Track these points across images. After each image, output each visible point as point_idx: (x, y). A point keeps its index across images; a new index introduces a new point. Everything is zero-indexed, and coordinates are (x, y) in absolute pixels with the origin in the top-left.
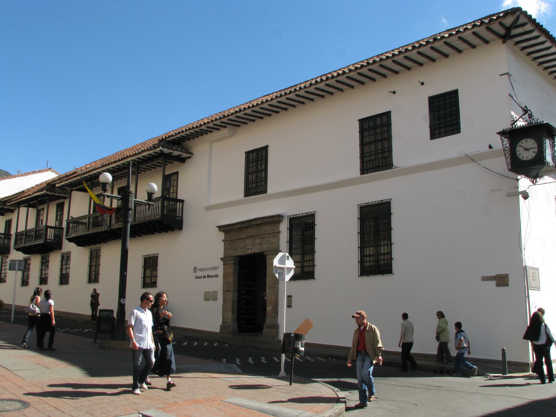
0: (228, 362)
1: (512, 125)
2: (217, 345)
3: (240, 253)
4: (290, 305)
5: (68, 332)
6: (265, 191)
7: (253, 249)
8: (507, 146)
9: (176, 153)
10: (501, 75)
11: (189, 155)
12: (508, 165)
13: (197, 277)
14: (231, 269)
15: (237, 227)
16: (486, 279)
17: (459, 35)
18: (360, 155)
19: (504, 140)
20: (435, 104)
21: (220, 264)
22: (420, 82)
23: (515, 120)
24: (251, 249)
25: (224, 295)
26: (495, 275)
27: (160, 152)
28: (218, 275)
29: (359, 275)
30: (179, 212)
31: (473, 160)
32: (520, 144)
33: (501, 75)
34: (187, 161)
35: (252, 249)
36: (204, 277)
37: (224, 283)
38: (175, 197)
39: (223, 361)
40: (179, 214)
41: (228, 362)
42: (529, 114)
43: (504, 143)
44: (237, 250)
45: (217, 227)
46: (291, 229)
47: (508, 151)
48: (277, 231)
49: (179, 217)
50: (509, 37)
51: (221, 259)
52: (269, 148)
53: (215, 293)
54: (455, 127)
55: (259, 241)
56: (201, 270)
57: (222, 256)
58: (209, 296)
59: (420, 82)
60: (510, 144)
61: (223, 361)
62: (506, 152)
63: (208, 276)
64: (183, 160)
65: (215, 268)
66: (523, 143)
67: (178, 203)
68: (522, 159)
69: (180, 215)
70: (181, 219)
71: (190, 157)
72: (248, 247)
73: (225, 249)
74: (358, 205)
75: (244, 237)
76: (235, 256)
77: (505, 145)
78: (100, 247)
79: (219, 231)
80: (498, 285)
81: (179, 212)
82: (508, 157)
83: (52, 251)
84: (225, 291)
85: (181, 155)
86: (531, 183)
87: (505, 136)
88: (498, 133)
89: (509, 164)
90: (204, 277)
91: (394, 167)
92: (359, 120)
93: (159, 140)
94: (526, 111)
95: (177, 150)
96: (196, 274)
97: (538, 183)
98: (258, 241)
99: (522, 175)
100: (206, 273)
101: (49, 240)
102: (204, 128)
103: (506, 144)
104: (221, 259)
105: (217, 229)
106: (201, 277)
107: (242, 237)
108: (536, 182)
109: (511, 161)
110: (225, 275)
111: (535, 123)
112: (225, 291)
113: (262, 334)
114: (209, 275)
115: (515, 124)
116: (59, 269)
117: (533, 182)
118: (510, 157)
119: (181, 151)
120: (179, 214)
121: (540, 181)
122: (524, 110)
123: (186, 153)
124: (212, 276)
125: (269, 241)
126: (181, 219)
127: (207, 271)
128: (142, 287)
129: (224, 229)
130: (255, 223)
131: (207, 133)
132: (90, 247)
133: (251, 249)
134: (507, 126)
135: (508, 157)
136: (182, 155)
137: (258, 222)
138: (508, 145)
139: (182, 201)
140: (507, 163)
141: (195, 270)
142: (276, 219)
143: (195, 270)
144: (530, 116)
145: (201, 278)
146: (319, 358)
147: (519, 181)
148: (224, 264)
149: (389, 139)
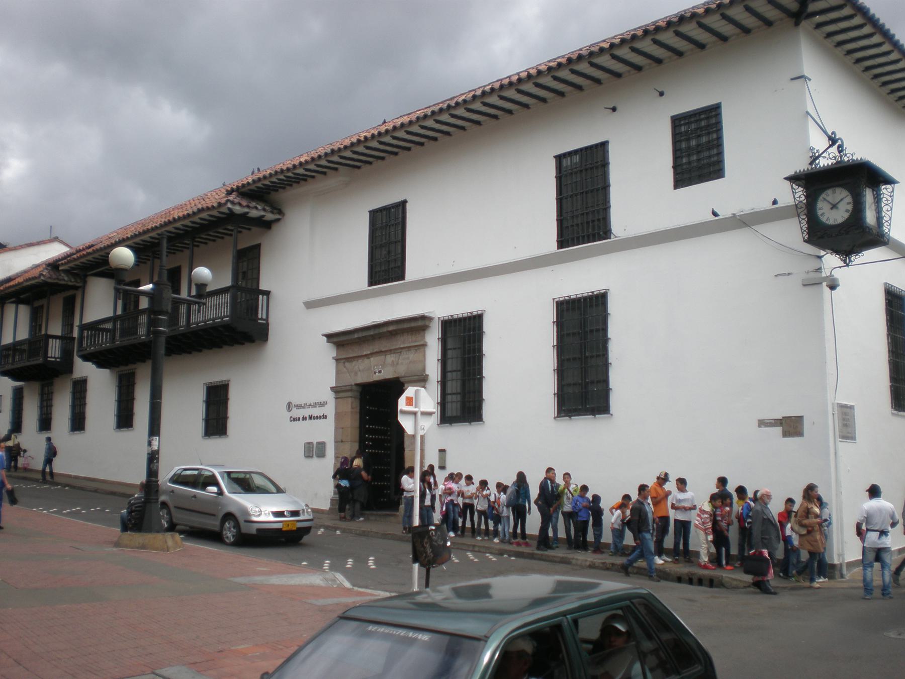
0: (332, 568)
1: (811, 164)
2: (323, 532)
3: (363, 378)
4: (443, 465)
5: (76, 515)
6: (402, 277)
7: (382, 372)
8: (801, 199)
9: (254, 213)
10: (792, 79)
11: (278, 216)
12: (803, 233)
13: (292, 419)
15: (356, 336)
16: (762, 423)
17: (721, 11)
18: (557, 216)
19: (797, 191)
20: (683, 129)
21: (330, 397)
22: (658, 91)
23: (817, 154)
24: (380, 372)
25: (336, 448)
26: (781, 418)
27: (227, 211)
28: (326, 416)
29: (556, 416)
30: (262, 311)
31: (744, 223)
32: (823, 195)
33: (792, 79)
34: (275, 227)
35: (381, 373)
36: (304, 418)
37: (336, 428)
38: (254, 287)
39: (324, 568)
40: (262, 314)
41: (332, 568)
42: (839, 147)
43: (797, 195)
44: (356, 374)
45: (323, 335)
46: (444, 340)
47: (802, 210)
48: (422, 343)
49: (262, 319)
50: (805, 14)
51: (332, 388)
52: (407, 204)
53: (322, 446)
54: (717, 167)
55: (392, 359)
56: (298, 407)
57: (334, 385)
58: (314, 450)
59: (658, 91)
60: (806, 197)
61: (324, 568)
62: (799, 211)
63: (311, 417)
64: (267, 225)
65: (322, 404)
66: (828, 195)
67: (261, 296)
68: (827, 222)
69: (264, 317)
70: (265, 322)
71: (278, 220)
72: (374, 368)
73: (338, 373)
74: (554, 299)
75: (369, 352)
76: (353, 384)
77: (798, 199)
78: (135, 369)
79: (328, 342)
80: (786, 434)
81: (262, 311)
82: (803, 219)
83: (57, 376)
84: (338, 442)
85: (263, 216)
86: (842, 264)
87: (798, 182)
88: (786, 179)
89: (805, 231)
90: (304, 418)
91: (612, 236)
92: (555, 157)
93: (227, 191)
94: (833, 140)
95: (256, 208)
96: (290, 414)
97: (853, 263)
98: (390, 358)
99: (827, 250)
100: (307, 412)
101: (51, 357)
102: (301, 171)
103: (800, 197)
104: (332, 388)
105: (325, 338)
106: (299, 418)
107: (365, 353)
108: (850, 261)
109: (808, 226)
110: (338, 416)
111: (848, 161)
112: (338, 442)
113: (398, 513)
114: (312, 415)
115: (817, 162)
116: (36, 420)
117: (845, 261)
118: (806, 219)
119: (264, 210)
120: (262, 314)
121: (857, 259)
122: (830, 138)
123: (272, 212)
124: (317, 416)
125: (408, 358)
126: (265, 322)
127: (309, 409)
128: (203, 435)
129: (335, 340)
130: (385, 329)
131: (306, 180)
132: (117, 369)
133: (380, 372)
134: (801, 165)
135: (803, 219)
136: (265, 216)
137: (391, 328)
138: (803, 198)
139: (267, 293)
140: (801, 228)
141: (289, 406)
142: (420, 323)
143: (289, 407)
144: (841, 149)
146: (487, 555)
147: (823, 259)
148: (336, 398)
149: (606, 187)
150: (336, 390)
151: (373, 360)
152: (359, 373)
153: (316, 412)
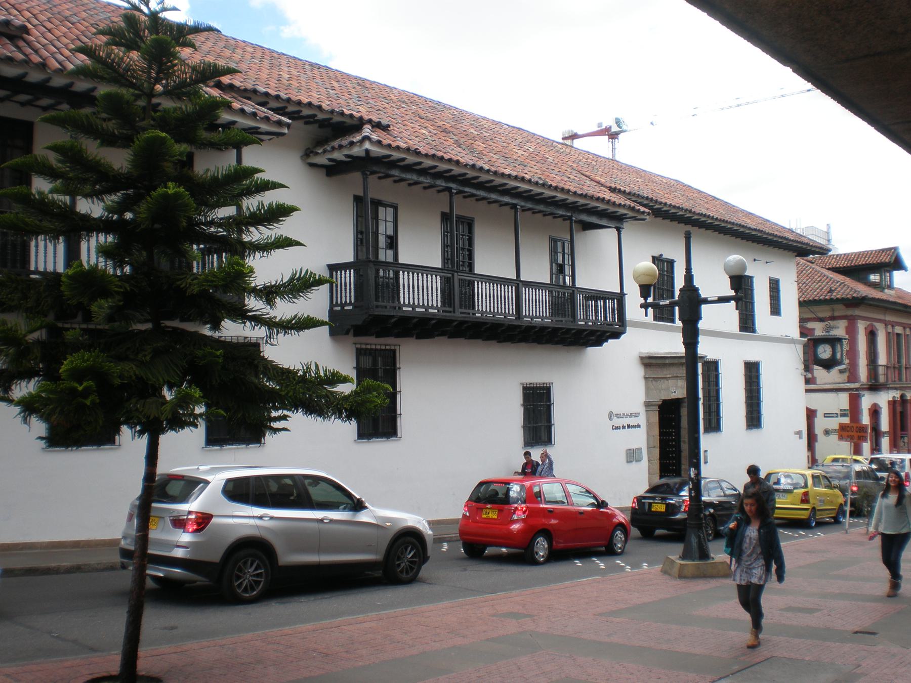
14: (655, 418)
21: (642, 410)
24: (675, 392)
56: (618, 416)
58: (632, 456)
63: (629, 426)
65: (636, 415)
73: (648, 390)
90: (624, 427)
112: (649, 448)
133: (675, 392)
141: (610, 417)
145: (620, 429)
150: (647, 405)
151: (671, 382)
152: (662, 391)
153: (632, 421)
